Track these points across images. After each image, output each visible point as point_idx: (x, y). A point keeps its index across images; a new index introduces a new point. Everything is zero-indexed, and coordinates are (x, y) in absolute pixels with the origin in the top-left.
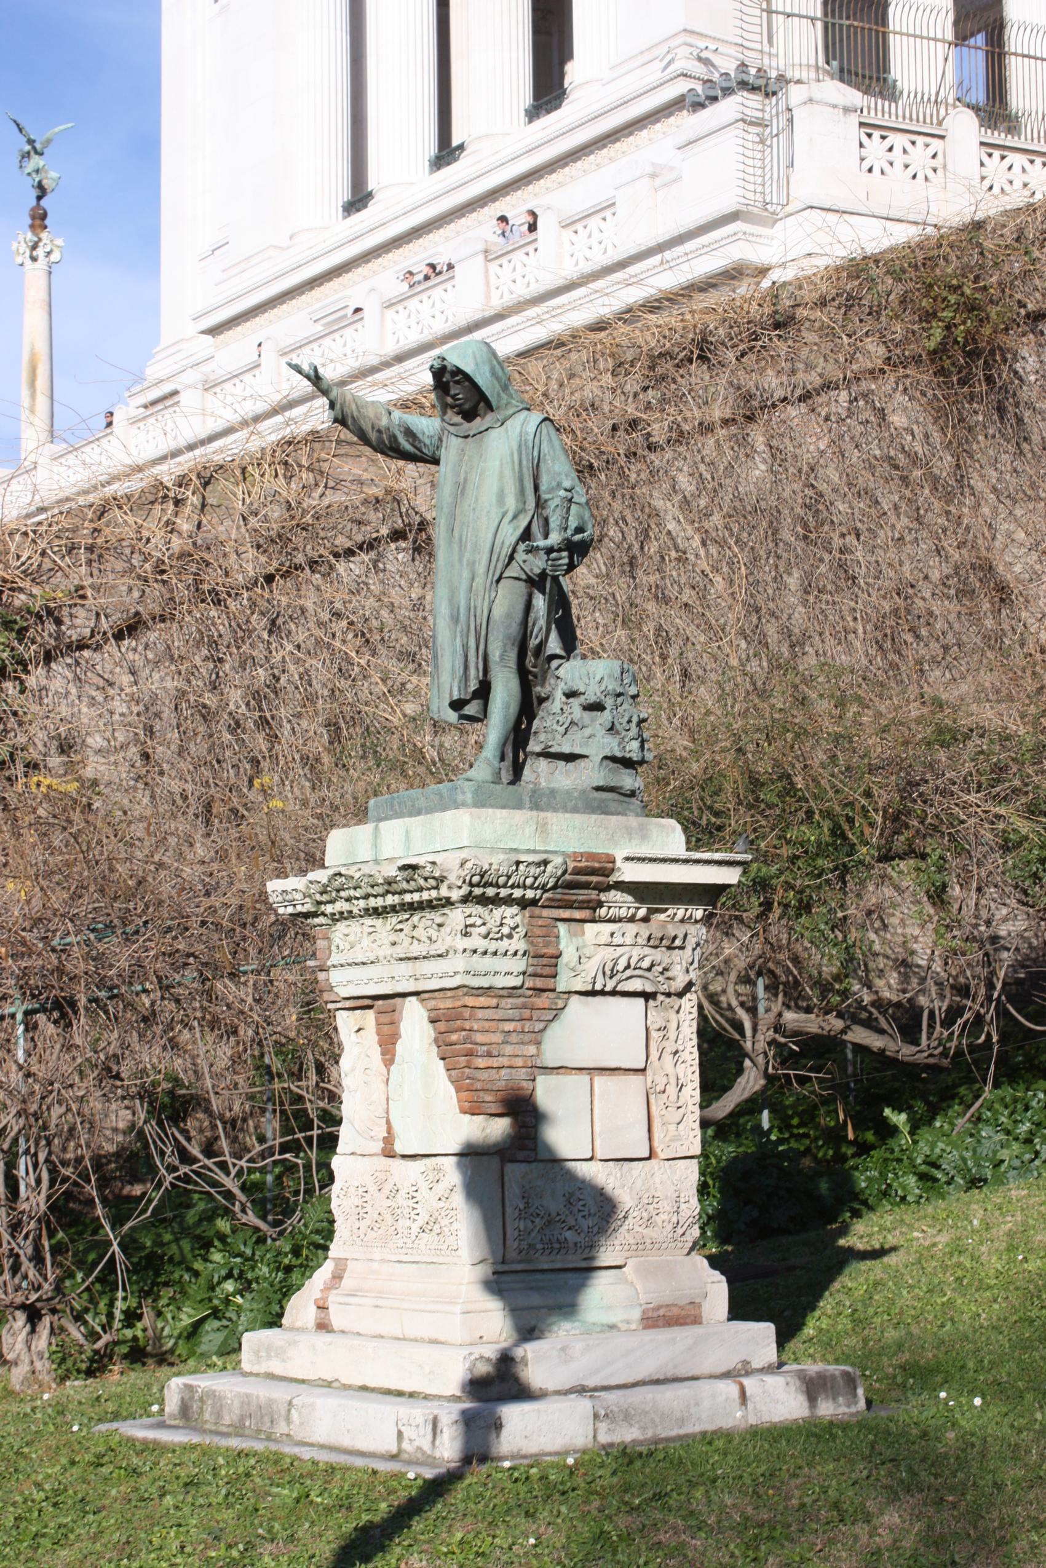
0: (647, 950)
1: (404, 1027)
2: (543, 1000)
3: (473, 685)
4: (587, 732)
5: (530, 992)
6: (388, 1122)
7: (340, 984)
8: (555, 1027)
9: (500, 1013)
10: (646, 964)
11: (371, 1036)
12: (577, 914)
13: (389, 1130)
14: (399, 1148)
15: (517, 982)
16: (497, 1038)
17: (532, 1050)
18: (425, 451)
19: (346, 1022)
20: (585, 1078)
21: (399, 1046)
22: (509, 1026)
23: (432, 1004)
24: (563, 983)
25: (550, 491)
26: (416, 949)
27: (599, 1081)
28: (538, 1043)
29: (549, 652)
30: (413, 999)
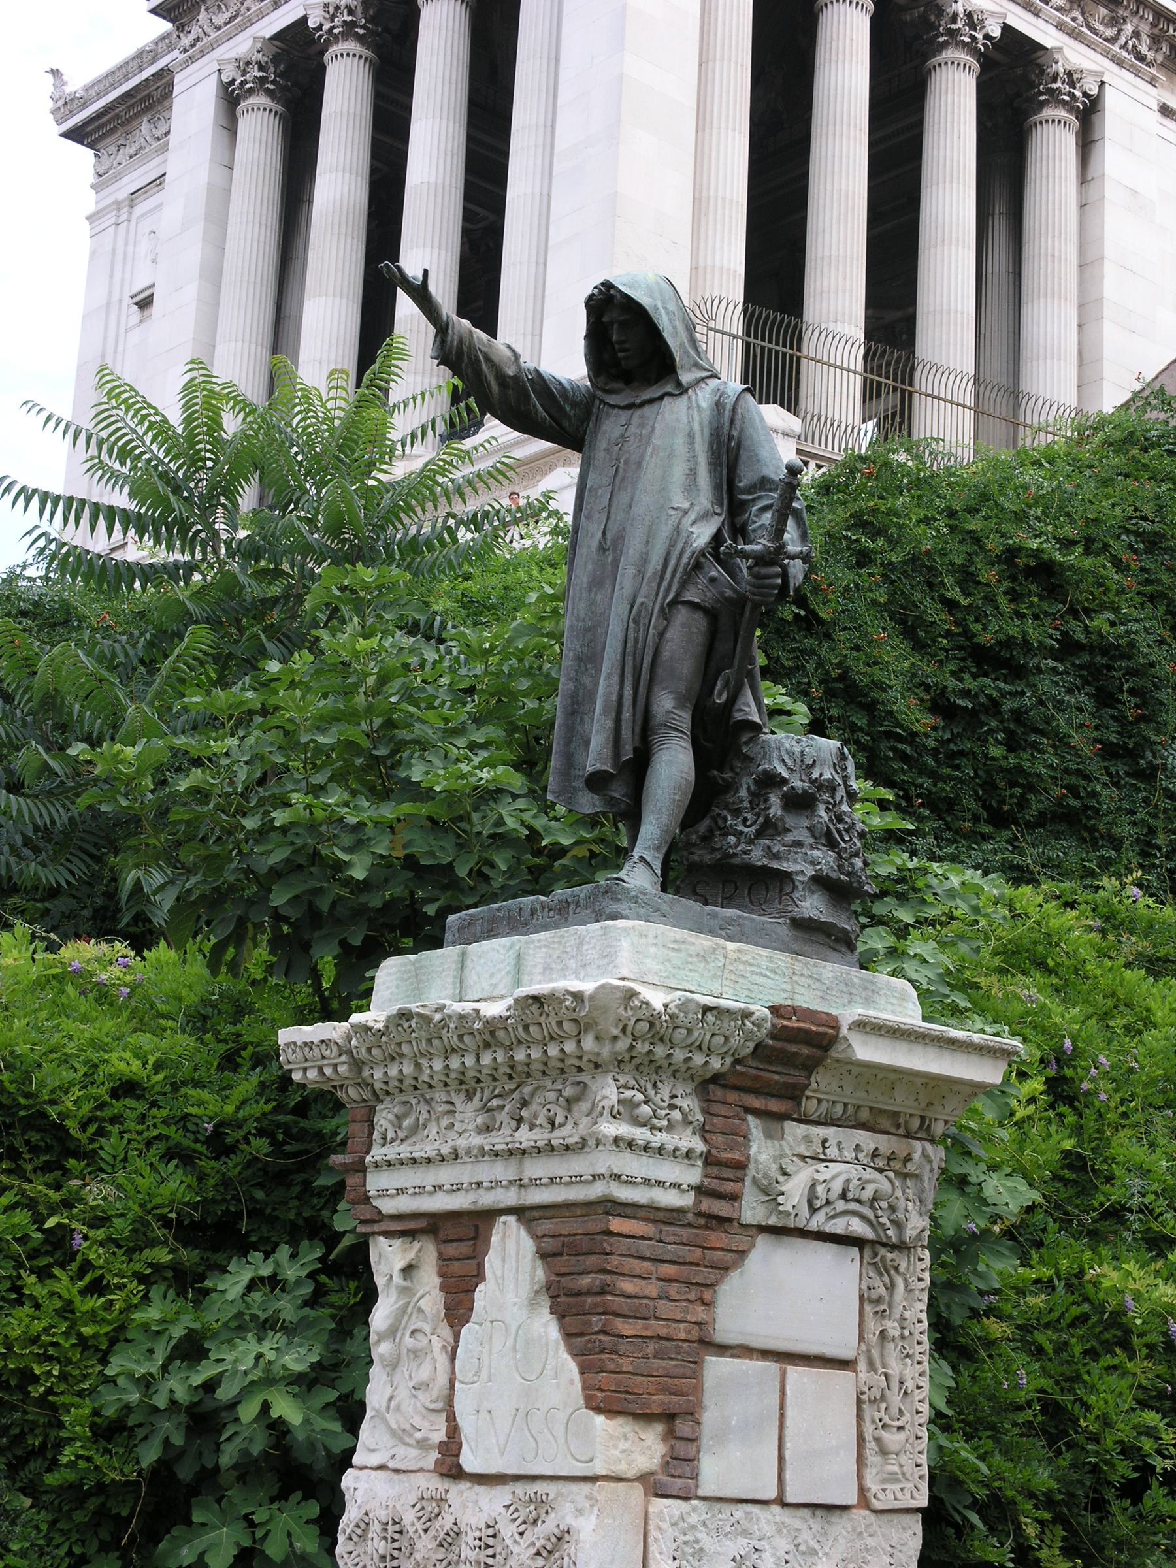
0: (870, 1174)
1: (492, 1262)
2: (717, 1238)
3: (628, 754)
4: (789, 838)
5: (702, 1221)
6: (451, 1418)
7: (383, 1193)
8: (734, 1277)
9: (660, 1251)
10: (867, 1194)
11: (429, 1281)
12: (774, 1105)
13: (453, 1431)
14: (470, 1461)
15: (687, 1200)
16: (652, 1288)
17: (700, 1313)
18: (566, 424)
19: (388, 1258)
20: (773, 1367)
21: (482, 1294)
22: (670, 1270)
23: (546, 1226)
24: (752, 1210)
25: (750, 489)
26: (525, 1137)
27: (795, 1373)
28: (708, 1305)
29: (739, 716)
30: (511, 1219)
